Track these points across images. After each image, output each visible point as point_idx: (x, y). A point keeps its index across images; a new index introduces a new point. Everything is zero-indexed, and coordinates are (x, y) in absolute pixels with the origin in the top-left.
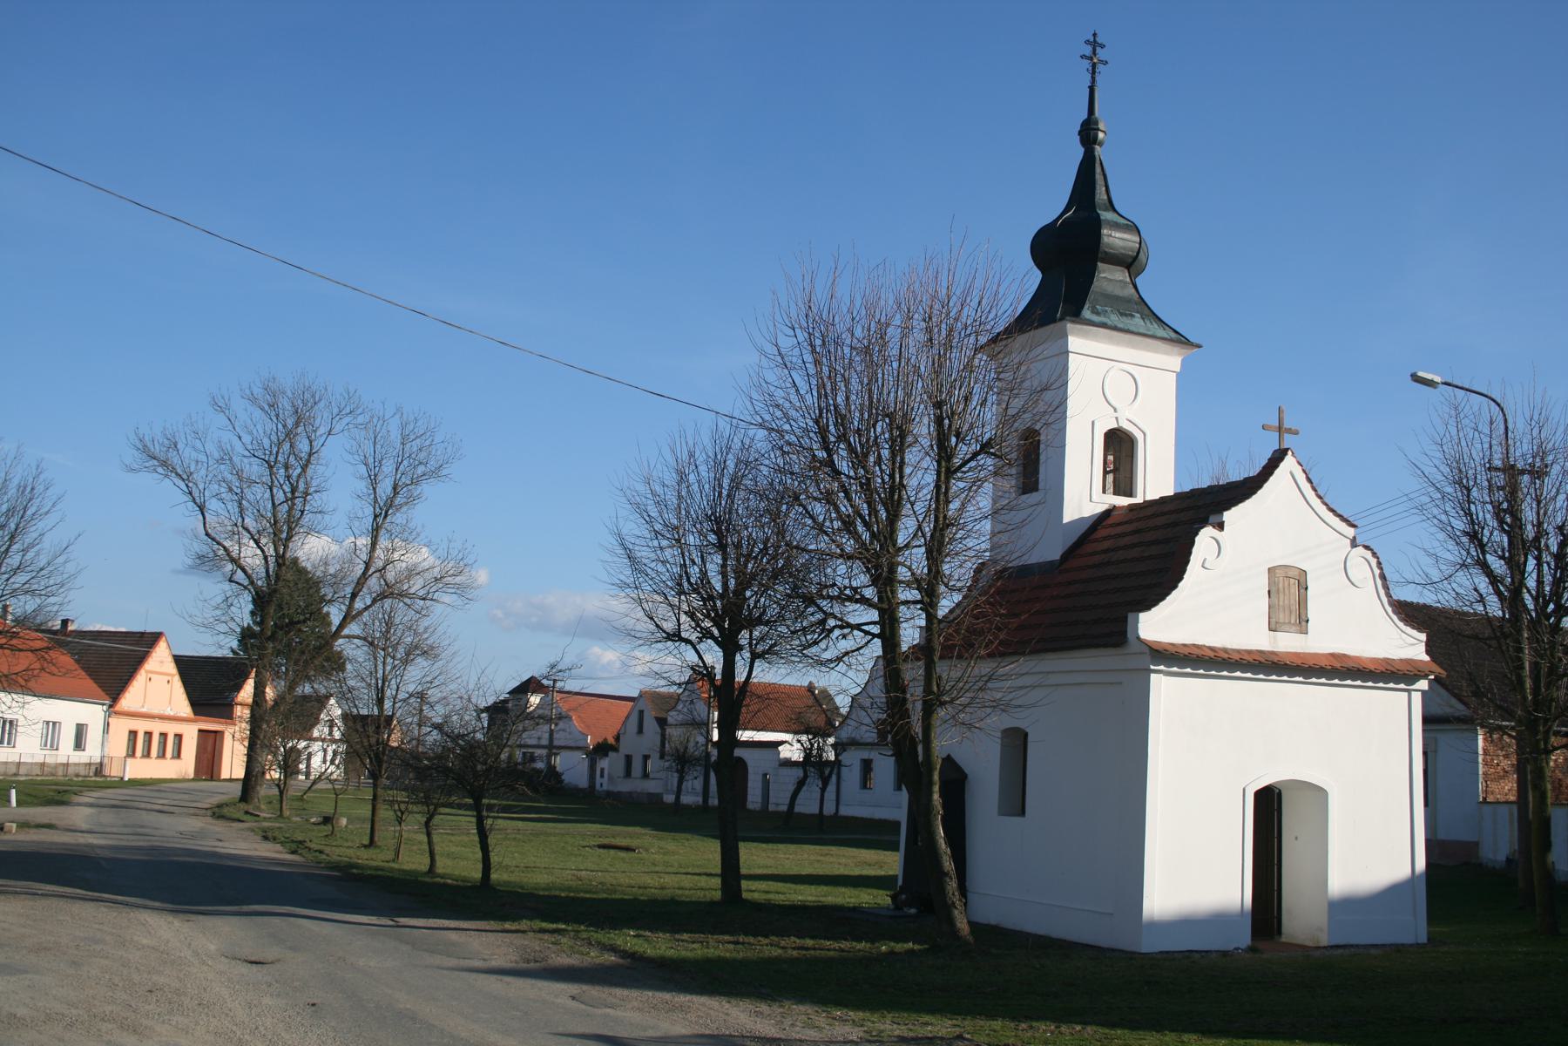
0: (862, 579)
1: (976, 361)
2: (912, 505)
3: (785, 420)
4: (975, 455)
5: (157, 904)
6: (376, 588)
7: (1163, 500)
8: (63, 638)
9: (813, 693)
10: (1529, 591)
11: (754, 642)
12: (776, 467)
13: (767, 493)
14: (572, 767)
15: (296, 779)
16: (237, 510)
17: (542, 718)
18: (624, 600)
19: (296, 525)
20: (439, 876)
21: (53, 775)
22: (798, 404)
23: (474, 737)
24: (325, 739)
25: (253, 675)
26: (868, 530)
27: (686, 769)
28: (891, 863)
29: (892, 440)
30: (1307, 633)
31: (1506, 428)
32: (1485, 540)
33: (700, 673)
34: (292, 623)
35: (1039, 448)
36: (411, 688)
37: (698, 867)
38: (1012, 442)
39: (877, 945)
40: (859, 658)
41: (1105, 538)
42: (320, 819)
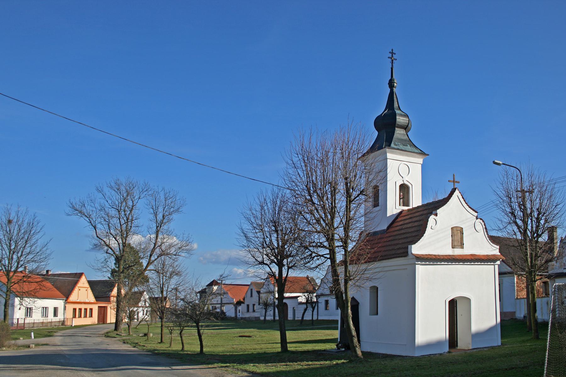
0: (323, 239)
1: (358, 163)
2: (339, 213)
3: (296, 186)
4: (358, 195)
5: (87, 369)
6: (159, 252)
7: (418, 207)
8: (47, 277)
9: (308, 279)
10: (529, 230)
11: (289, 263)
12: (294, 203)
13: (291, 212)
14: (229, 311)
15: (134, 321)
16: (108, 227)
17: (218, 294)
18: (244, 252)
19: (129, 232)
20: (185, 351)
21: (46, 326)
22: (300, 181)
23: (195, 302)
24: (143, 306)
25: (117, 286)
26: (325, 222)
27: (267, 308)
28: (336, 334)
29: (332, 191)
30: (463, 248)
31: (521, 178)
32: (516, 214)
33: (271, 275)
34: (129, 266)
35: (379, 192)
36: (173, 287)
37: (273, 340)
38: (370, 191)
39: (332, 361)
40: (323, 266)
41: (401, 221)
42: (143, 335)
